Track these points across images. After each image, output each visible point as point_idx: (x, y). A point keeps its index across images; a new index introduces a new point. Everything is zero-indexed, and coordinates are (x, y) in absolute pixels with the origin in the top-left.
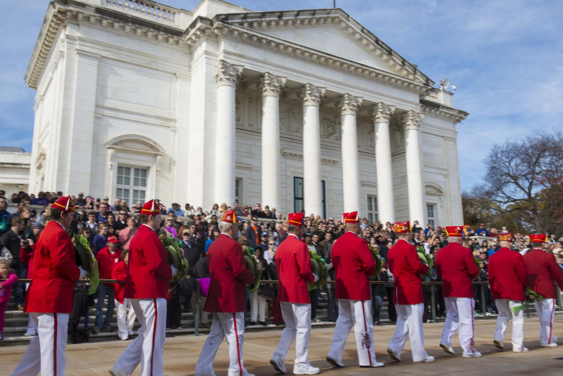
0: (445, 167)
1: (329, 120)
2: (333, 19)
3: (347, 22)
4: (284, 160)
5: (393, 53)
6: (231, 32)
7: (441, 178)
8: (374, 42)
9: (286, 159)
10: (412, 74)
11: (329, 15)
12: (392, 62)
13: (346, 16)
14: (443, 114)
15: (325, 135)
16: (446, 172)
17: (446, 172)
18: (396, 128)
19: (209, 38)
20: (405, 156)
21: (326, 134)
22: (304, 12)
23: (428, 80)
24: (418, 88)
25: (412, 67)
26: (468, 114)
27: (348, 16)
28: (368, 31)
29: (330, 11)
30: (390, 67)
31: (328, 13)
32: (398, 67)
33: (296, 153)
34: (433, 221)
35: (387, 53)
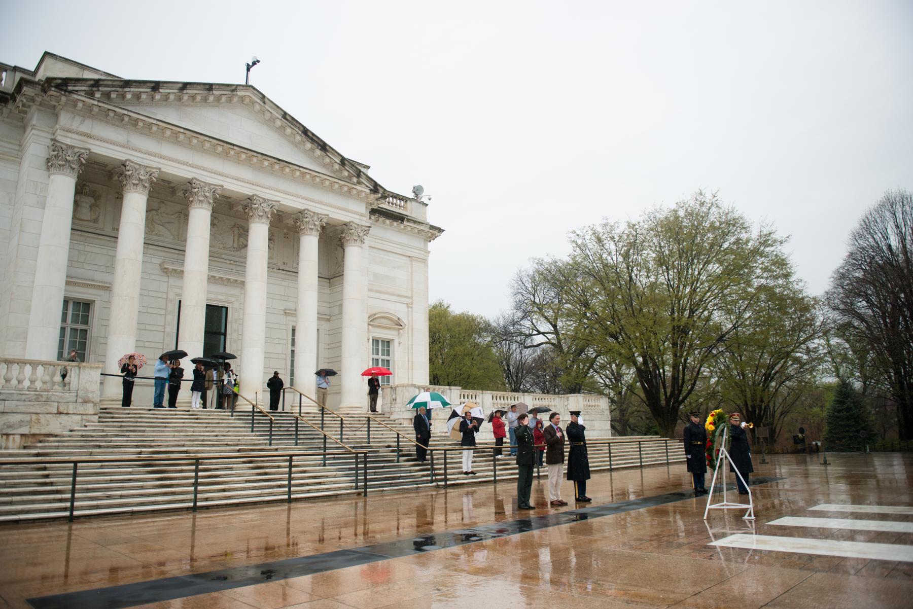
0: (410, 295)
1: (243, 228)
2: (242, 99)
3: (261, 103)
4: (167, 278)
5: (328, 148)
6: (75, 104)
7: (403, 308)
8: (301, 133)
9: (168, 276)
11: (235, 93)
12: (327, 160)
13: (261, 96)
14: (409, 228)
15: (234, 248)
16: (409, 301)
17: (409, 301)
18: (339, 243)
19: (41, 108)
20: (343, 279)
21: (235, 245)
22: (195, 86)
24: (364, 195)
25: (354, 168)
26: (443, 231)
27: (264, 96)
28: (293, 118)
30: (324, 166)
31: (233, 91)
32: (337, 167)
33: (174, 268)
34: (388, 361)
35: (320, 148)
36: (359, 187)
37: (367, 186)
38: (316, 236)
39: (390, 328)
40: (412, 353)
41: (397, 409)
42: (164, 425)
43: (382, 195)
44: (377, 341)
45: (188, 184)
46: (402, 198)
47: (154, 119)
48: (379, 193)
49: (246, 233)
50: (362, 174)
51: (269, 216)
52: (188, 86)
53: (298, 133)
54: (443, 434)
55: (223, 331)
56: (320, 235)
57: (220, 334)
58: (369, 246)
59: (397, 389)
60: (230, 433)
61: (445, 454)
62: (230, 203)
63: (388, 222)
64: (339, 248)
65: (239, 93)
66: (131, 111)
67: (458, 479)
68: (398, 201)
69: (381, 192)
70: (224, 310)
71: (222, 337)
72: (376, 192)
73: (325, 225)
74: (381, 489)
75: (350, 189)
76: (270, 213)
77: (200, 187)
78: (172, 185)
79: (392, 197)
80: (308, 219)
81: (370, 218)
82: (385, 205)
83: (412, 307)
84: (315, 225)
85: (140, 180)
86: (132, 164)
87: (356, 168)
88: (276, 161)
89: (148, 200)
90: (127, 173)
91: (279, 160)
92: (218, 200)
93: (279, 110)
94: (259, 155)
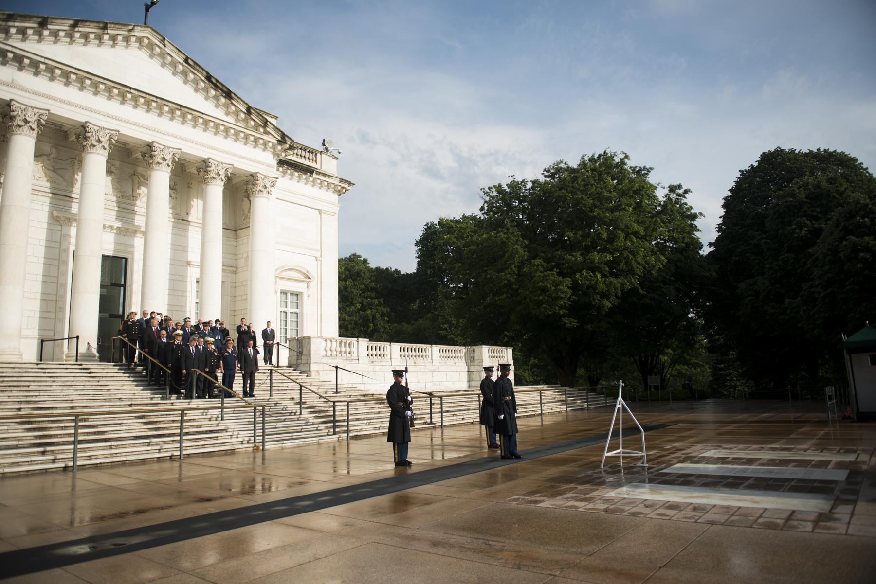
3: (161, 46)
5: (233, 95)
8: (203, 78)
10: (261, 126)
11: (133, 33)
13: (160, 38)
23: (283, 136)
24: (270, 145)
25: (261, 118)
26: (354, 184)
27: (164, 39)
28: (195, 63)
29: (133, 28)
32: (243, 116)
34: (297, 314)
35: (224, 95)
36: (266, 137)
37: (274, 137)
38: (221, 186)
39: (299, 281)
40: (321, 306)
41: (304, 361)
42: (53, 379)
43: (290, 146)
44: (286, 294)
45: (81, 128)
46: (312, 151)
47: (42, 57)
48: (286, 143)
49: (146, 182)
50: (268, 123)
51: (170, 164)
52: (80, 24)
53: (201, 79)
54: (350, 386)
55: (123, 283)
56: (225, 185)
57: (121, 286)
58: (277, 199)
59: (304, 341)
60: (125, 387)
61: (348, 405)
62: (129, 150)
63: (296, 174)
64: (246, 199)
65: (136, 34)
66: (15, 47)
67: (361, 430)
68: (307, 154)
69: (289, 143)
70: (124, 260)
71: (122, 289)
72: (284, 143)
73: (229, 175)
74: (282, 442)
75: (256, 140)
76: (171, 161)
77: (94, 131)
78: (65, 129)
79: (301, 149)
80: (211, 169)
81: (278, 170)
82: (292, 157)
83: (321, 261)
84: (219, 174)
85: (26, 122)
86: (18, 105)
87: (263, 117)
88: (177, 107)
89: (36, 143)
90: (12, 113)
91: (180, 106)
92: (113, 145)
93: (182, 55)
94: (159, 100)
